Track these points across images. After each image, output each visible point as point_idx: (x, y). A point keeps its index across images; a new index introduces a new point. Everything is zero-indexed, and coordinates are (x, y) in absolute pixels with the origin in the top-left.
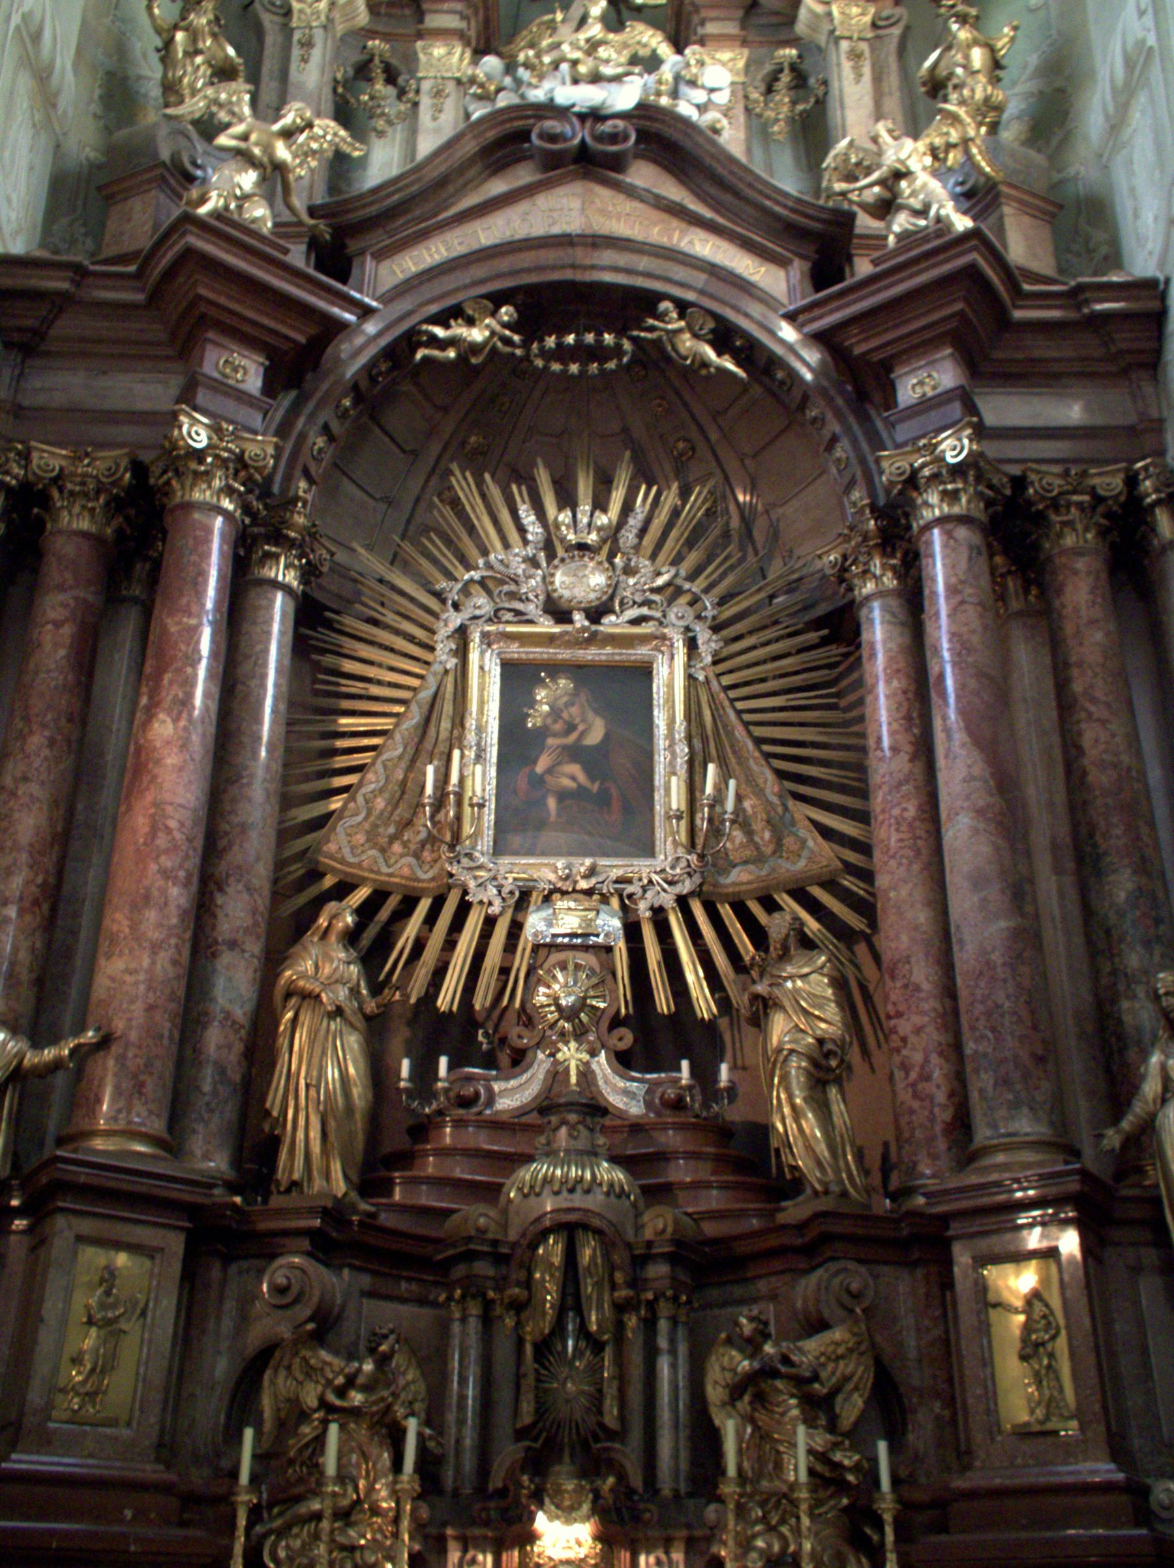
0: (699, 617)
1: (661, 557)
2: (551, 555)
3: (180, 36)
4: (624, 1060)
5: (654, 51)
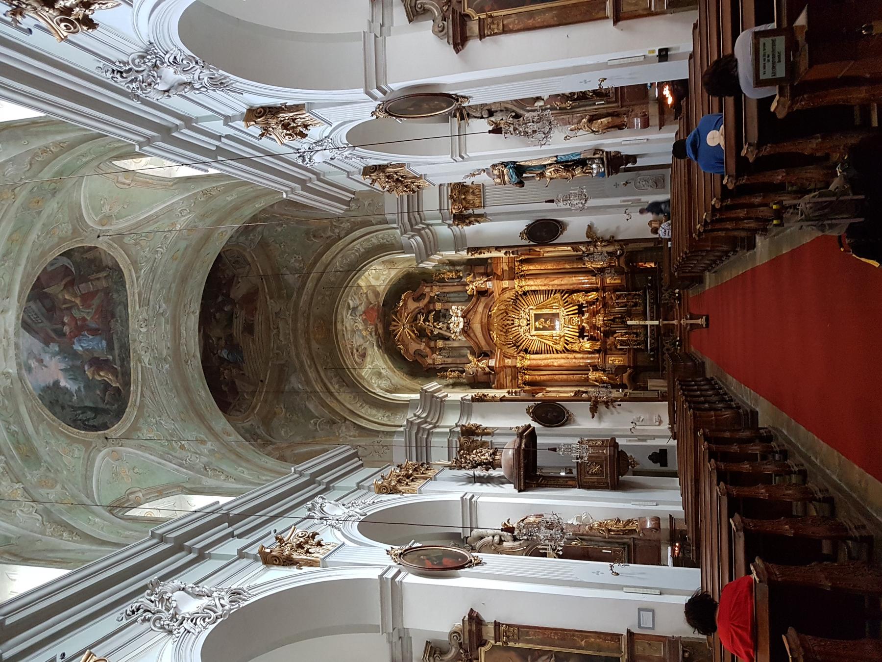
4: (583, 315)
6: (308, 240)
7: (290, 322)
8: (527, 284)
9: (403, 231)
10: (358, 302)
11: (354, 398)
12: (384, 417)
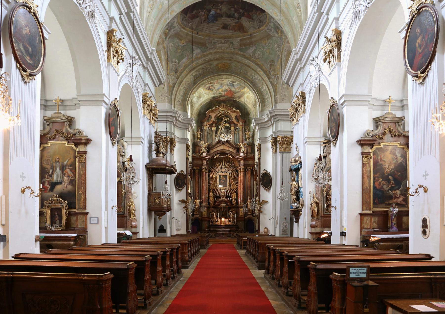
4: (226, 198)
6: (269, 61)
7: (228, 50)
8: (242, 172)
9: (271, 112)
10: (236, 87)
11: (188, 84)
12: (179, 99)
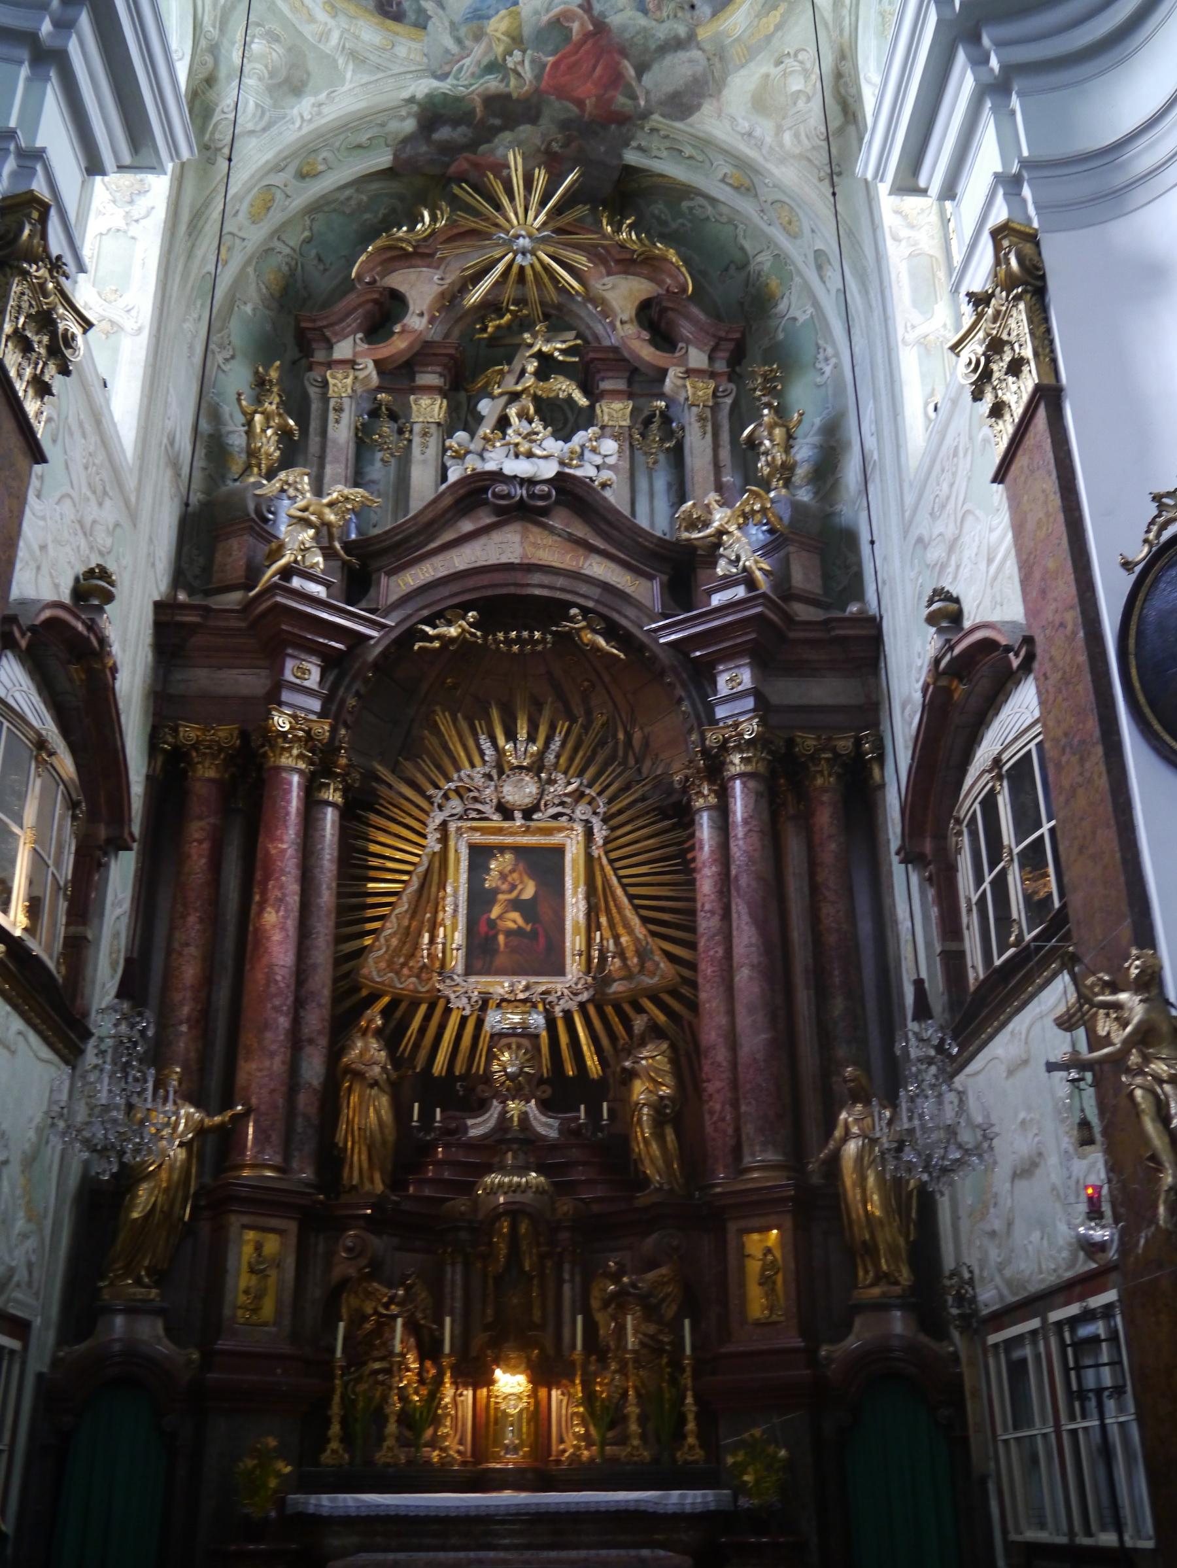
0: (595, 813)
1: (571, 772)
2: (501, 772)
3: (258, 418)
4: (546, 1106)
5: (570, 395)
